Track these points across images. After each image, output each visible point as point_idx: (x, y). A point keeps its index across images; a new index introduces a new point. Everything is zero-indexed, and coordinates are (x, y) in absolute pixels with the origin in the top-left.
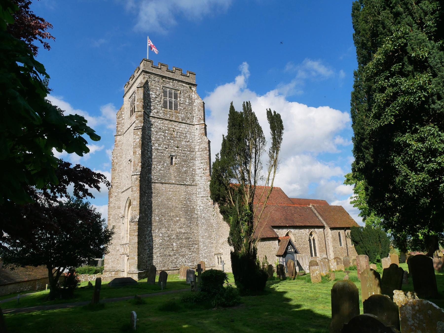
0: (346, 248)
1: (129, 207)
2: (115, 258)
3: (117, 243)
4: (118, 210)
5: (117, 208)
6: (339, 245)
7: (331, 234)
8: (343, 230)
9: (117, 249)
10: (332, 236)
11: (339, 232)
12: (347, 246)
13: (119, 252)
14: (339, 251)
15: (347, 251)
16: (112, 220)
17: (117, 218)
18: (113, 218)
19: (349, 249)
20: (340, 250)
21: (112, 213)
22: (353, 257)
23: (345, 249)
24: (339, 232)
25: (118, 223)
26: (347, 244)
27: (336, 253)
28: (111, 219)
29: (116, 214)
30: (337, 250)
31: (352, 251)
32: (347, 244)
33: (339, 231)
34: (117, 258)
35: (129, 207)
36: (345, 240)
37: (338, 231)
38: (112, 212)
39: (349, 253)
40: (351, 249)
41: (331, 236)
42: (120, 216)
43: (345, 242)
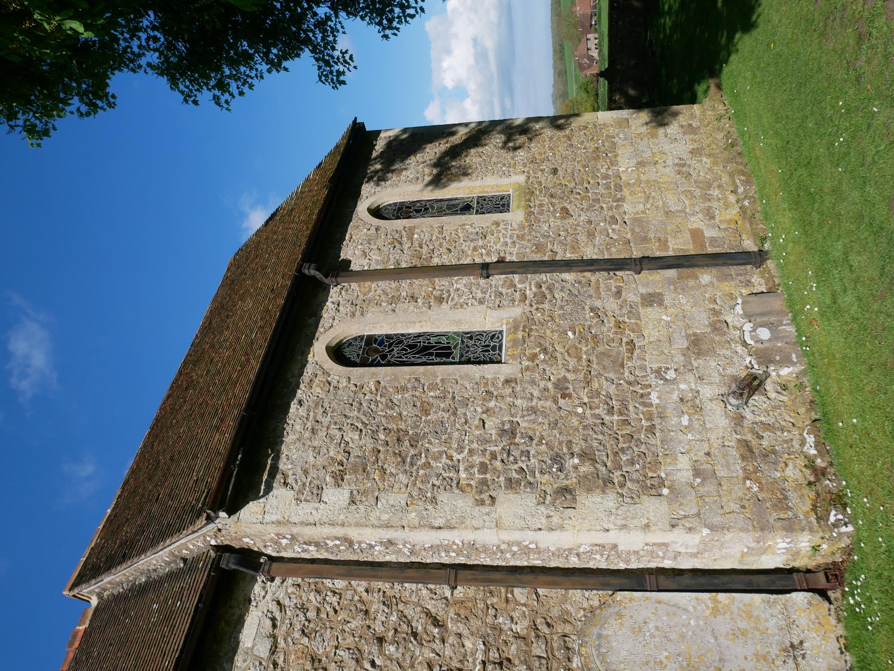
0: (528, 284)
6: (488, 370)
7: (318, 492)
8: (334, 292)
10: (339, 479)
11: (338, 353)
12: (503, 266)
14: (562, 389)
15: (568, 276)
19: (539, 247)
20: (556, 372)
22: (626, 207)
23: (541, 297)
24: (338, 353)
26: (485, 269)
27: (585, 456)
30: (541, 429)
31: (566, 212)
32: (485, 269)
33: (318, 353)
36: (442, 283)
37: (309, 369)
39: (590, 253)
40: (550, 224)
41: (336, 497)
43: (461, 283)
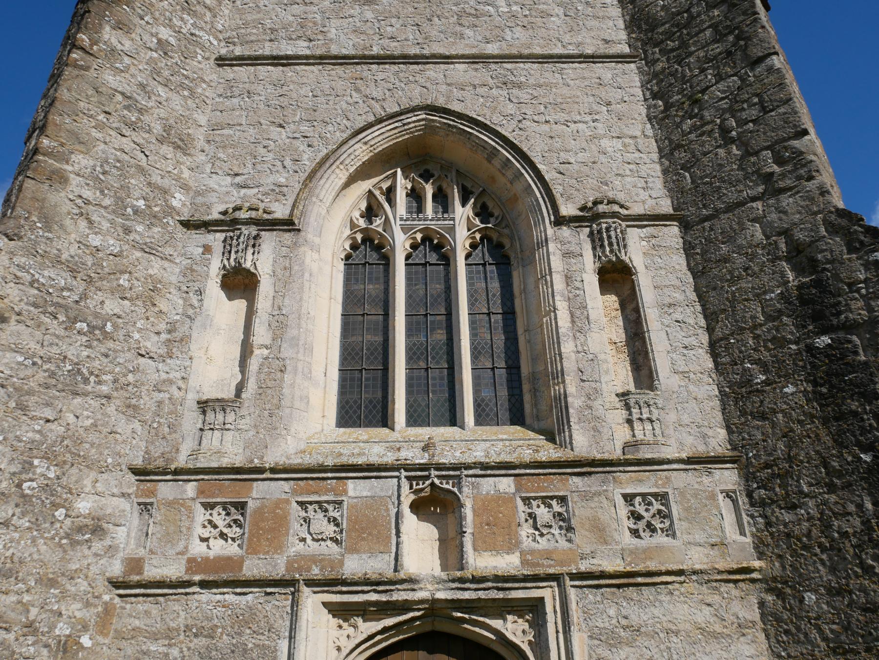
1: (347, 184)
2: (30, 627)
3: (92, 437)
4: (167, 150)
5: (157, 128)
9: (83, 506)
13: (98, 546)
16: (87, 194)
17: (141, 203)
18: (96, 180)
21: (95, 133)
25: (149, 250)
28: (74, 180)
29: (141, 170)
34: (62, 629)
35: (347, 184)
38: (99, 127)
42: (175, 203)
